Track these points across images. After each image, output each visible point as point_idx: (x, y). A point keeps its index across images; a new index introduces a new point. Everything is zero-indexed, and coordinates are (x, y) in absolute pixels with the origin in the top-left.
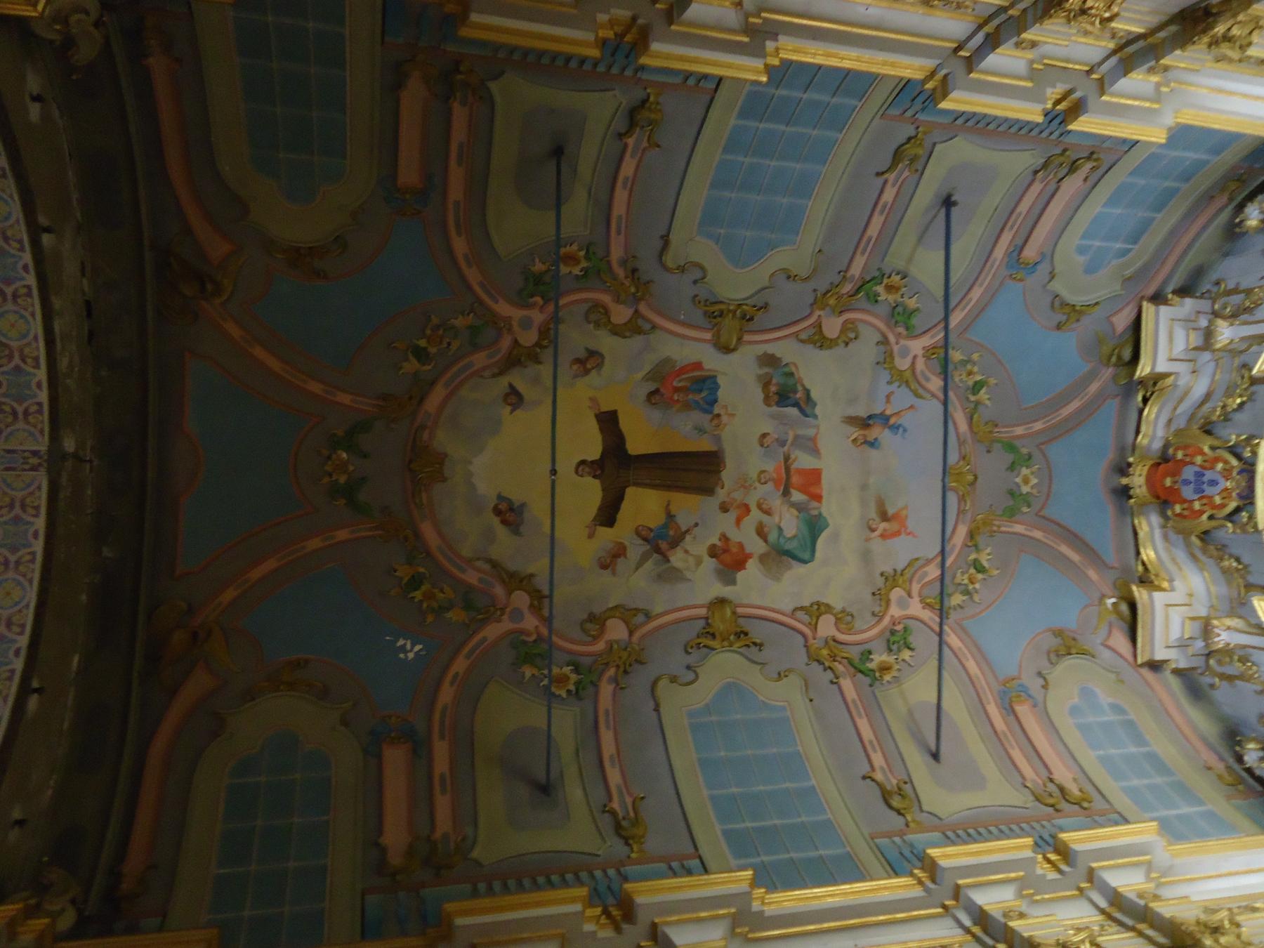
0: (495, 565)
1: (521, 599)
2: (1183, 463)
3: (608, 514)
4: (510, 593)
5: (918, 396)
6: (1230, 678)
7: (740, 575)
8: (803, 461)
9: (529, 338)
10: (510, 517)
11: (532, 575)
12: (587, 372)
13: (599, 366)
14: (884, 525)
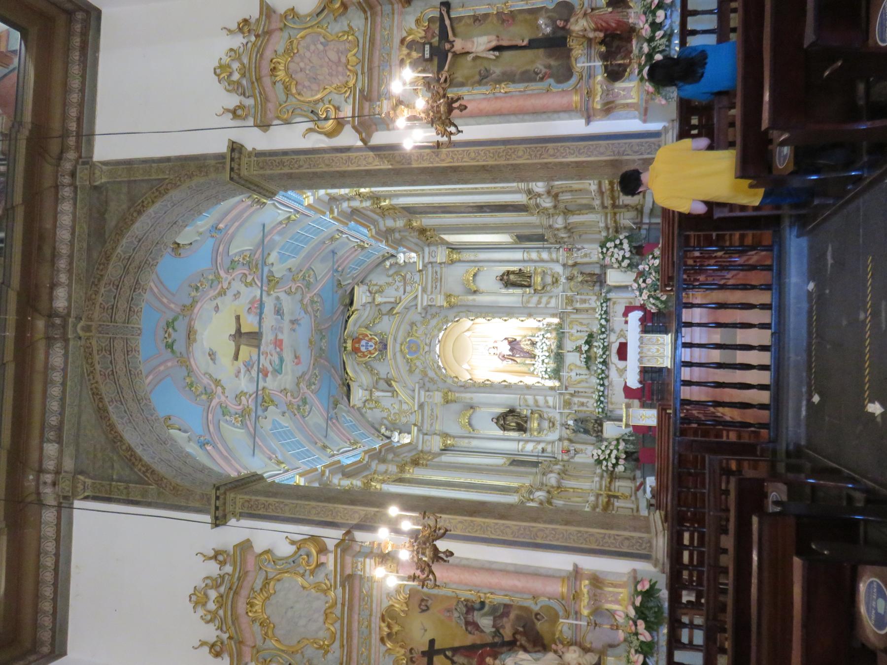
0: (211, 376)
1: (219, 389)
2: (362, 339)
3: (236, 357)
4: (216, 388)
5: (305, 313)
6: (371, 409)
7: (267, 379)
8: (280, 337)
9: (225, 286)
10: (213, 357)
11: (220, 380)
12: (236, 299)
13: (239, 297)
14: (296, 360)
